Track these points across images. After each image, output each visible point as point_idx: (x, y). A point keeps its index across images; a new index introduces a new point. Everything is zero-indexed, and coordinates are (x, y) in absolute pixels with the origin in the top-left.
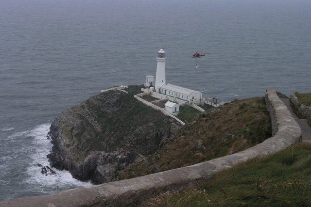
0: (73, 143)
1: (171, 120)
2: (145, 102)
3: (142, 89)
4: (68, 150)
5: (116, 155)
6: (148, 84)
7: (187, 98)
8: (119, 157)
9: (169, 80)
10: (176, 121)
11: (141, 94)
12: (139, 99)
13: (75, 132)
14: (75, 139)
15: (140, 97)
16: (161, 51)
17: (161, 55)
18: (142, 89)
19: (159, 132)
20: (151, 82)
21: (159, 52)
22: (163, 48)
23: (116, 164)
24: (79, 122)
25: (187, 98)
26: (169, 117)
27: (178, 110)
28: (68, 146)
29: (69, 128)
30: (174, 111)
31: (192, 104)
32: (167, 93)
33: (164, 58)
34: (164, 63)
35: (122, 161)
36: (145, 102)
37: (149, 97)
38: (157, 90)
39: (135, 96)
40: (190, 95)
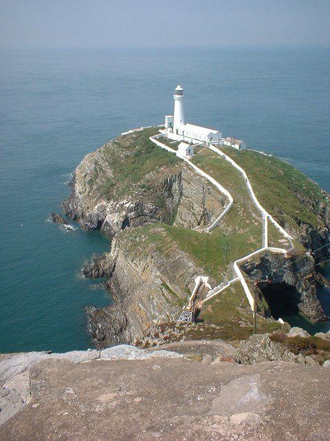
2: (159, 144)
3: (160, 131)
4: (81, 197)
5: (123, 204)
8: (127, 205)
10: (187, 165)
11: (157, 136)
13: (88, 178)
14: (87, 186)
16: (179, 88)
18: (160, 131)
23: (124, 213)
26: (182, 160)
27: (192, 152)
28: (81, 193)
32: (185, 134)
35: (130, 210)
36: (159, 144)
38: (175, 131)
39: (150, 138)
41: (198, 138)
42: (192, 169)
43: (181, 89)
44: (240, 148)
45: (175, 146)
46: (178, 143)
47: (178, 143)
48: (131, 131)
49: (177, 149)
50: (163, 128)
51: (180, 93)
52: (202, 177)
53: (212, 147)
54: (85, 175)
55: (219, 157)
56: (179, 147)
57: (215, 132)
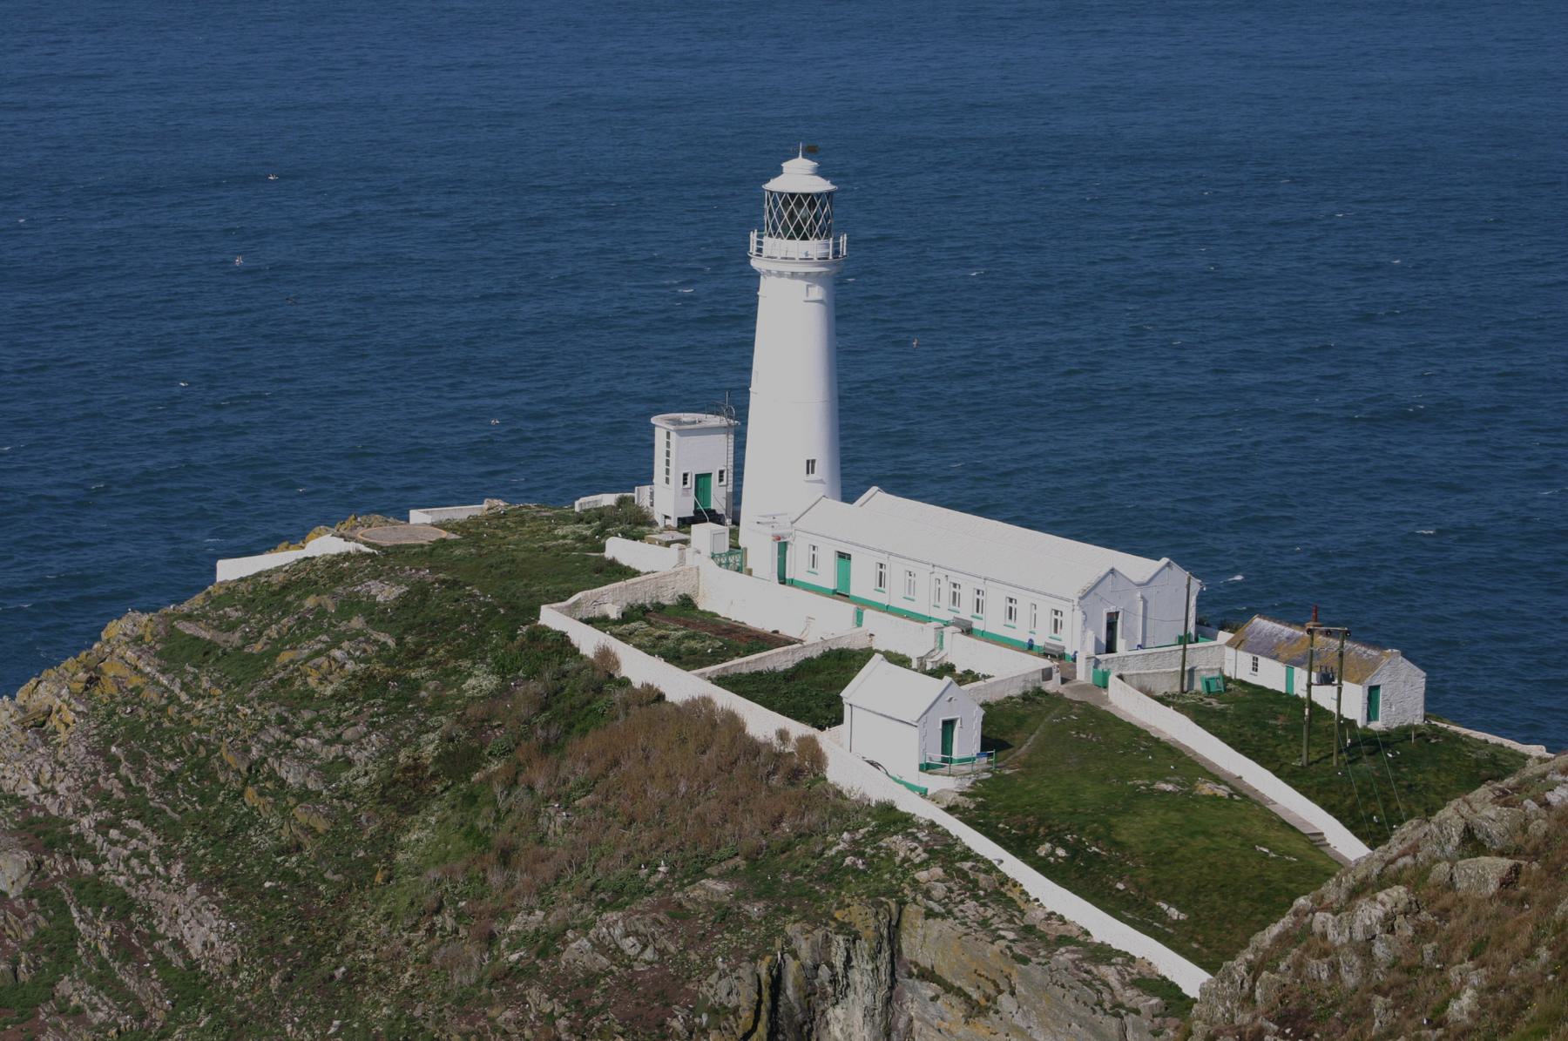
1: (899, 844)
2: (640, 668)
3: (617, 548)
9: (878, 445)
10: (945, 851)
11: (611, 600)
12: (588, 641)
15: (600, 622)
16: (798, 176)
18: (617, 548)
19: (792, 966)
20: (702, 480)
22: (810, 153)
26: (890, 818)
30: (937, 756)
32: (862, 585)
36: (640, 668)
39: (551, 617)
41: (993, 621)
42: (1002, 894)
43: (822, 185)
44: (1372, 714)
45: (816, 687)
46: (843, 663)
47: (843, 663)
48: (324, 545)
49: (829, 713)
50: (637, 524)
52: (1103, 954)
55: (1206, 788)
56: (850, 694)
57: (1137, 568)
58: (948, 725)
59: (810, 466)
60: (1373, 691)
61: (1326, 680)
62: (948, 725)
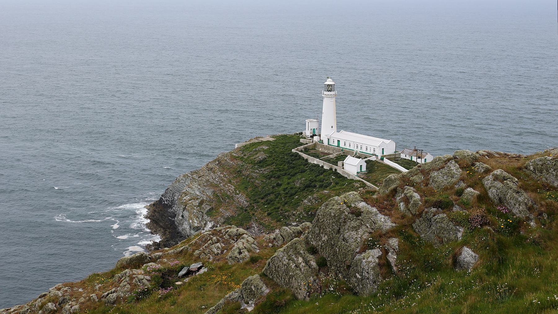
0: (205, 224)
6: (308, 133)
7: (374, 151)
15: (301, 151)
16: (329, 82)
17: (330, 88)
21: (327, 83)
24: (209, 193)
25: (374, 151)
27: (364, 169)
29: (197, 203)
30: (359, 171)
31: (382, 159)
33: (332, 93)
34: (334, 99)
37: (312, 150)
40: (378, 146)
51: (330, 88)
53: (387, 161)
54: (201, 203)
58: (361, 166)
59: (332, 127)
60: (425, 159)
61: (419, 158)
62: (361, 166)
